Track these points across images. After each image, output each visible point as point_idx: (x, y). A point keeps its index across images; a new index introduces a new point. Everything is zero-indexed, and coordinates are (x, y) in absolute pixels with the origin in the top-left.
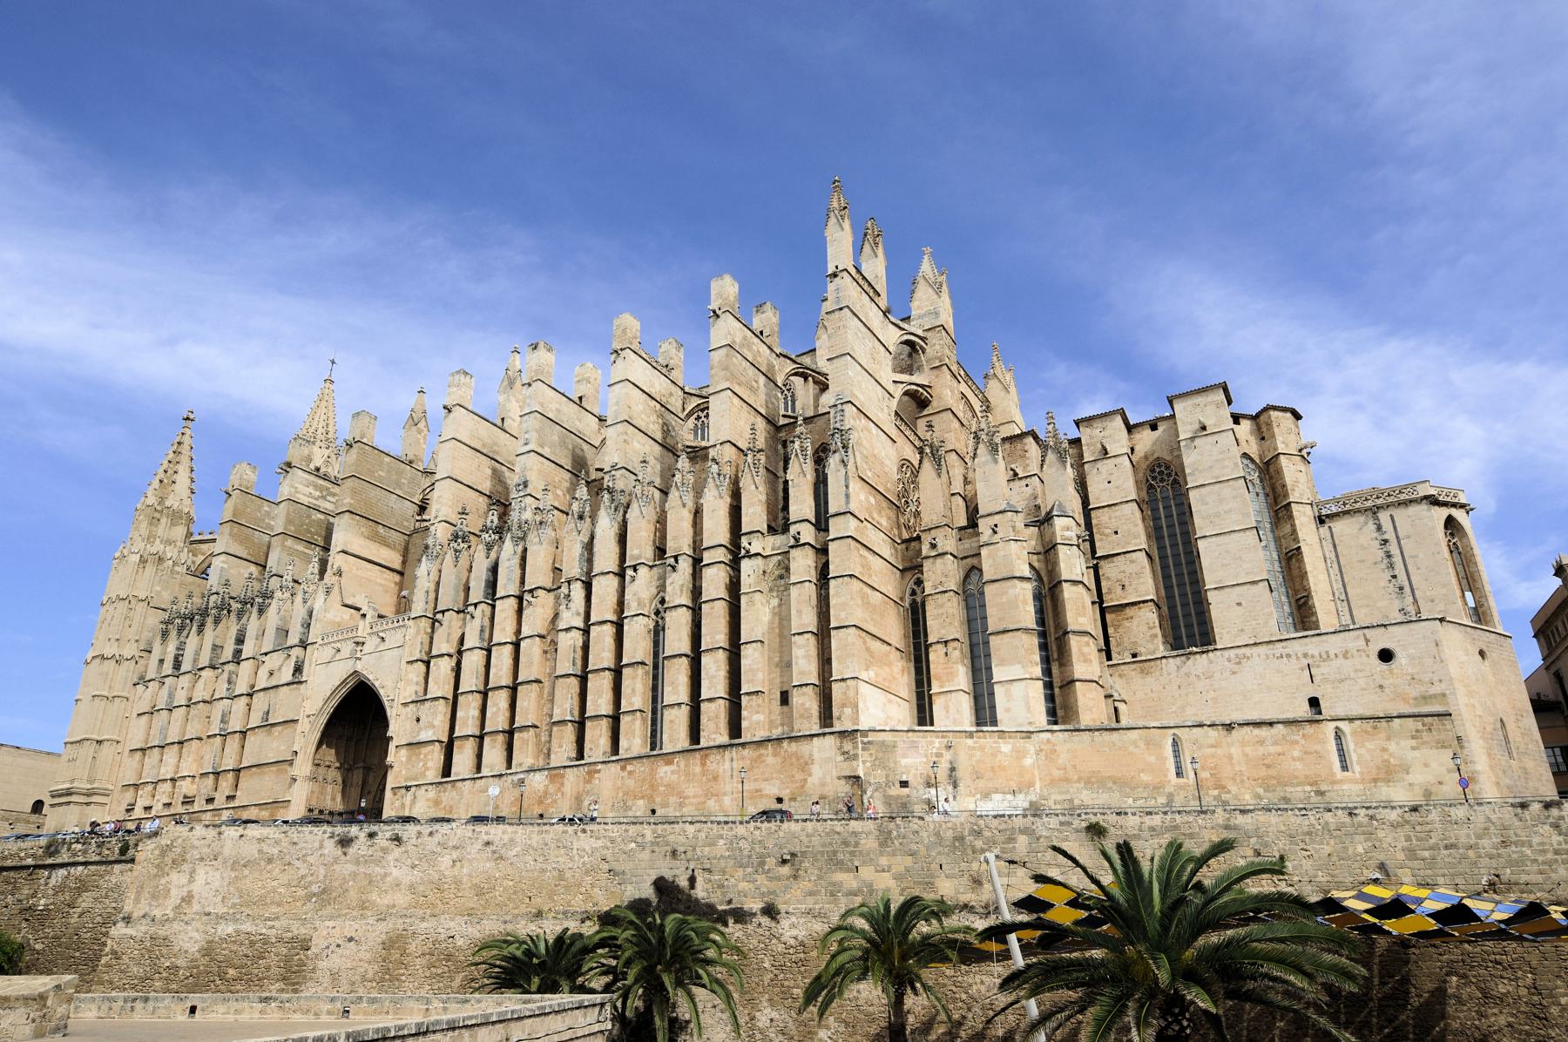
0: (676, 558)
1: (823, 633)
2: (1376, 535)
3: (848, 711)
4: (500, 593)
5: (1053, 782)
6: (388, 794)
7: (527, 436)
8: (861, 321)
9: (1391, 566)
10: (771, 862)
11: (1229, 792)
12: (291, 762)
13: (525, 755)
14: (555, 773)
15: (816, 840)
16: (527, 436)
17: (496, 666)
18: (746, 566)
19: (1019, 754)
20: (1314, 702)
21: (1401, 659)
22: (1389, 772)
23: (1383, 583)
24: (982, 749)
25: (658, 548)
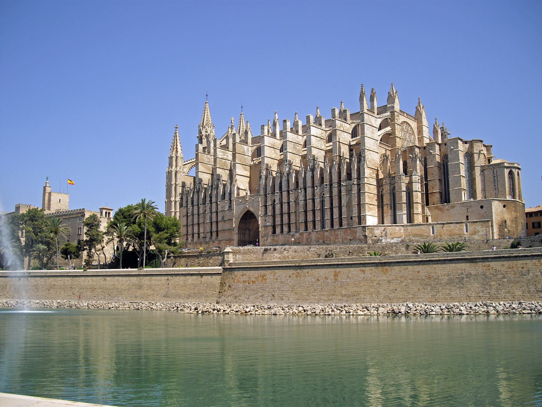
0: (326, 185)
1: (359, 205)
2: (493, 175)
3: (364, 222)
4: (283, 190)
5: (406, 236)
6: (260, 238)
7: (285, 147)
8: (369, 125)
9: (495, 183)
10: (348, 253)
11: (442, 237)
12: (233, 230)
13: (293, 229)
14: (301, 234)
15: (356, 248)
16: (285, 147)
17: (284, 208)
18: (343, 189)
19: (400, 230)
20: (467, 217)
21: (484, 208)
22: (475, 233)
23: (493, 187)
24: (392, 229)
25: (322, 178)
